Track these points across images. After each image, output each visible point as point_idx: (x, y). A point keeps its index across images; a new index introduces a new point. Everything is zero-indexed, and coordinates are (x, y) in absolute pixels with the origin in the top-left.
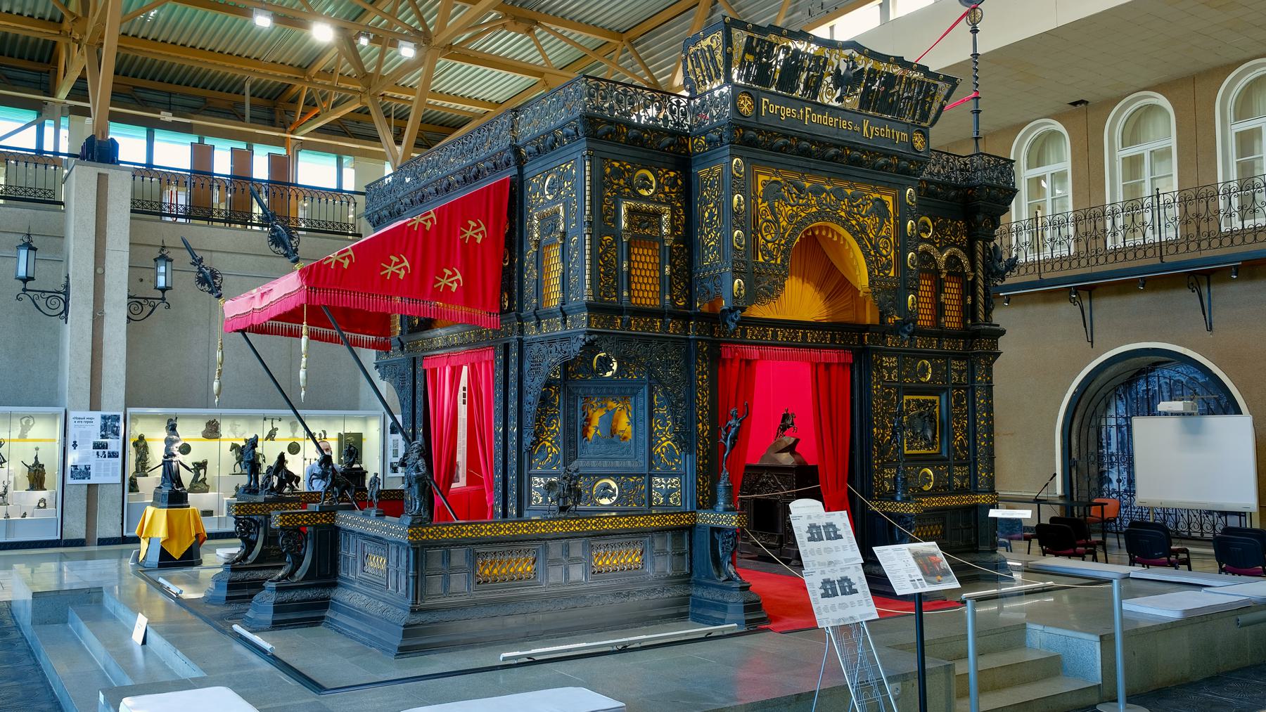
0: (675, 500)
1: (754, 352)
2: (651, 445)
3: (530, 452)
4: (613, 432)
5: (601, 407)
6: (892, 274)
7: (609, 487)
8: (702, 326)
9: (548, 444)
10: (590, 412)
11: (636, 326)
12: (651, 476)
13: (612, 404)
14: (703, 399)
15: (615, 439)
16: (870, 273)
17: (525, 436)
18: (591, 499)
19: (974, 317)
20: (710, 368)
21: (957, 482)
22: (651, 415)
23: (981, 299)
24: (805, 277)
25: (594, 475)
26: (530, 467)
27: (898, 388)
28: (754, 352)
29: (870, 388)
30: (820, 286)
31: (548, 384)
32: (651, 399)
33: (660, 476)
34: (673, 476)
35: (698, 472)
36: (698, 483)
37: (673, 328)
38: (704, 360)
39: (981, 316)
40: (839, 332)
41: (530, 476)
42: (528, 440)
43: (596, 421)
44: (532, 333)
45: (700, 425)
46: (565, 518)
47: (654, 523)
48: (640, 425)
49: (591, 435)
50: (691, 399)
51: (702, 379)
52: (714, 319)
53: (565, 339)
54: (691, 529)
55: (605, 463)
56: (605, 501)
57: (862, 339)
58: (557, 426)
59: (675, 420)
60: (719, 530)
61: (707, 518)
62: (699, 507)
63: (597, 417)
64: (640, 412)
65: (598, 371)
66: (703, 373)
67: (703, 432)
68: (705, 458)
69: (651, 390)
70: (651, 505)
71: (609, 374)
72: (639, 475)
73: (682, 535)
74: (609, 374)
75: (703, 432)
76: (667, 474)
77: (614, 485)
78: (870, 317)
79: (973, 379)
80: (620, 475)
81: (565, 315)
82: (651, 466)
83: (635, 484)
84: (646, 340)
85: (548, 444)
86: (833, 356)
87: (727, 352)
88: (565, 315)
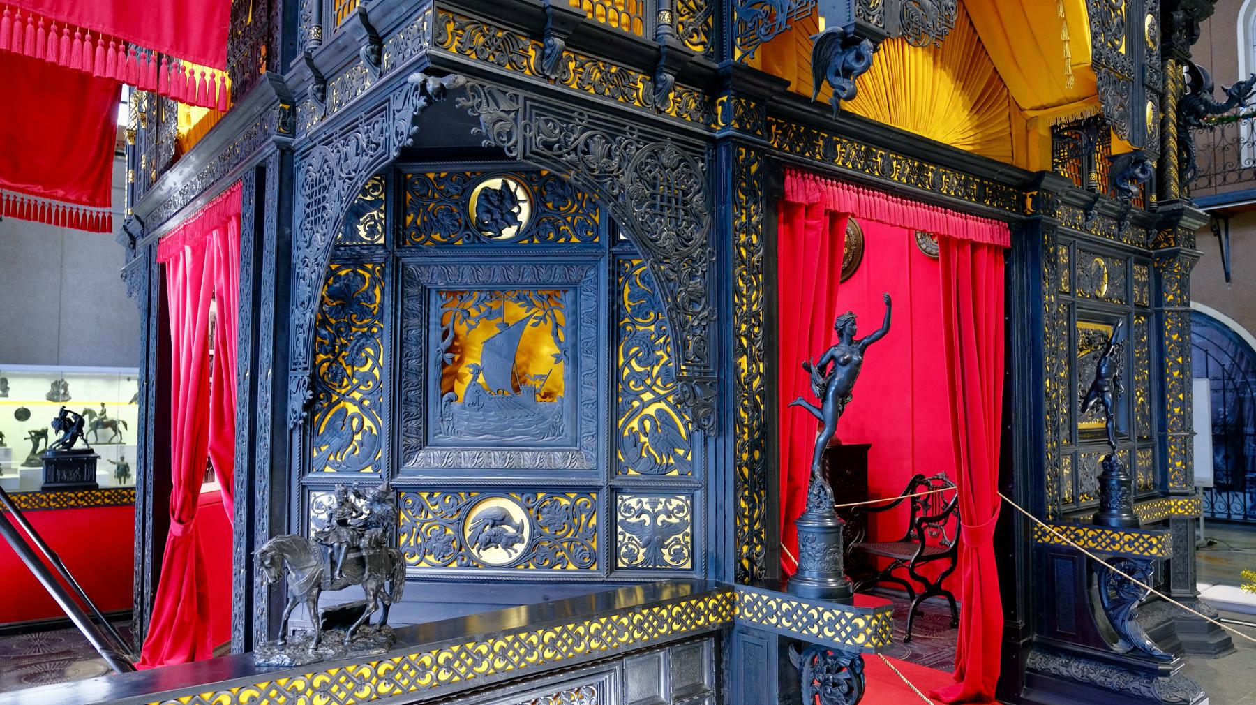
0: (677, 555)
1: (845, 198)
2: (615, 411)
3: (308, 427)
4: (517, 382)
5: (490, 314)
6: (1122, 50)
7: (504, 518)
8: (747, 110)
10: (462, 329)
11: (581, 76)
12: (615, 491)
13: (515, 311)
14: (751, 298)
15: (523, 396)
16: (1094, 36)
17: (292, 387)
18: (457, 550)
19: (1162, 189)
20: (765, 222)
21: (1141, 479)
22: (615, 336)
23: (1174, 159)
24: (938, 56)
25: (468, 489)
26: (306, 465)
27: (1070, 306)
28: (845, 198)
29: (1040, 298)
30: (963, 78)
31: (347, 254)
32: (615, 292)
33: (638, 492)
34: (671, 492)
35: (740, 481)
36: (739, 513)
37: (679, 106)
38: (751, 193)
39: (1174, 188)
40: (994, 182)
41: (305, 490)
42: (298, 397)
43: (475, 356)
44: (311, 121)
45: (743, 361)
46: (340, 661)
47: (626, 630)
48: (587, 362)
49: (461, 389)
50: (723, 292)
51: (749, 244)
52: (765, 97)
53: (379, 107)
54: (721, 637)
55: (496, 458)
56: (496, 556)
57: (1022, 200)
58: (374, 364)
59: (681, 348)
60: (800, 646)
61: (763, 610)
62: (748, 578)
63: (478, 340)
64: (588, 332)
65: (481, 226)
66: (748, 228)
67: (751, 377)
68: (754, 445)
69: (617, 271)
70: (613, 567)
71: (509, 233)
72: (584, 490)
73: (697, 651)
74: (509, 233)
75: (751, 377)
76: (657, 486)
77: (518, 514)
78: (1038, 158)
79: (1159, 300)
80: (535, 489)
81: (377, 41)
82: (614, 467)
83: (572, 512)
84: (613, 122)
85: (352, 409)
86: (979, 230)
87: (799, 190)
88: (377, 41)
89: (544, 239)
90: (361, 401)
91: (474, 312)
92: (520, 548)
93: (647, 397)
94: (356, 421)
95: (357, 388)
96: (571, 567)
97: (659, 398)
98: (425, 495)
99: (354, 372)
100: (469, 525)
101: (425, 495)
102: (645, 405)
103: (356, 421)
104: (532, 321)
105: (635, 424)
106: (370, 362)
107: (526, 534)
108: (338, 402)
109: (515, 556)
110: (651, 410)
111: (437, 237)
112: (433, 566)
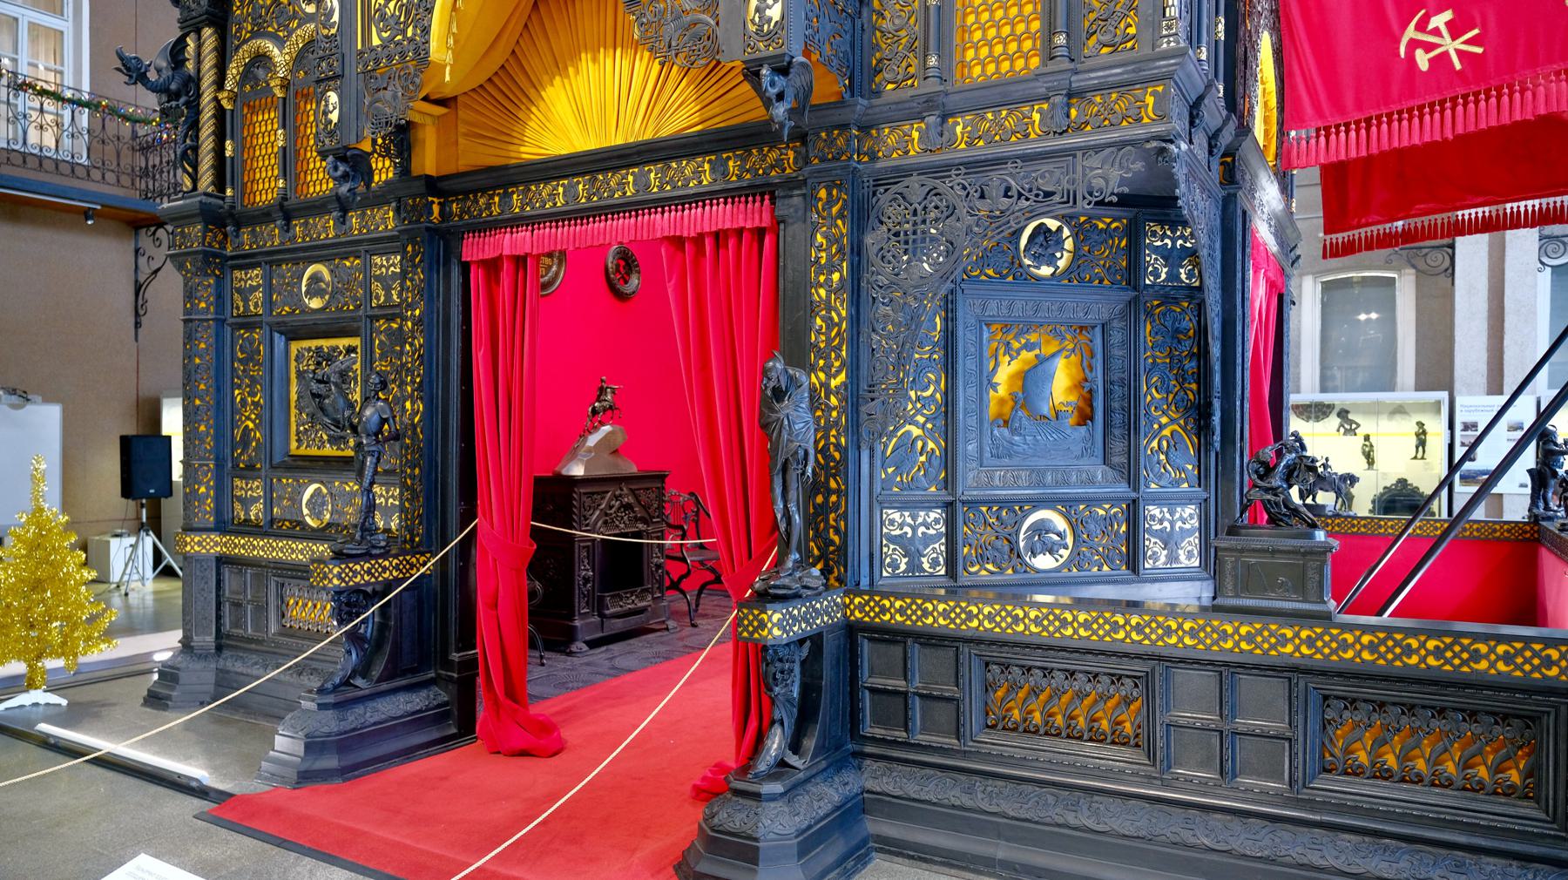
9: (916, 432)
56: (1044, 562)
77: (1060, 523)
89: (1081, 280)
90: (924, 425)
91: (1016, 345)
92: (1065, 553)
93: (1164, 420)
94: (920, 444)
95: (918, 412)
96: (1105, 568)
97: (1172, 421)
98: (984, 509)
99: (918, 399)
100: (1022, 536)
101: (984, 509)
102: (1162, 427)
103: (920, 444)
104: (1065, 353)
105: (1155, 444)
106: (932, 388)
107: (1069, 540)
108: (903, 426)
109: (1061, 561)
110: (1166, 432)
111: (990, 272)
112: (992, 573)
